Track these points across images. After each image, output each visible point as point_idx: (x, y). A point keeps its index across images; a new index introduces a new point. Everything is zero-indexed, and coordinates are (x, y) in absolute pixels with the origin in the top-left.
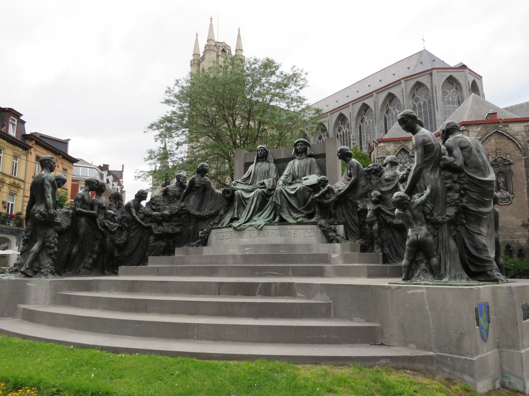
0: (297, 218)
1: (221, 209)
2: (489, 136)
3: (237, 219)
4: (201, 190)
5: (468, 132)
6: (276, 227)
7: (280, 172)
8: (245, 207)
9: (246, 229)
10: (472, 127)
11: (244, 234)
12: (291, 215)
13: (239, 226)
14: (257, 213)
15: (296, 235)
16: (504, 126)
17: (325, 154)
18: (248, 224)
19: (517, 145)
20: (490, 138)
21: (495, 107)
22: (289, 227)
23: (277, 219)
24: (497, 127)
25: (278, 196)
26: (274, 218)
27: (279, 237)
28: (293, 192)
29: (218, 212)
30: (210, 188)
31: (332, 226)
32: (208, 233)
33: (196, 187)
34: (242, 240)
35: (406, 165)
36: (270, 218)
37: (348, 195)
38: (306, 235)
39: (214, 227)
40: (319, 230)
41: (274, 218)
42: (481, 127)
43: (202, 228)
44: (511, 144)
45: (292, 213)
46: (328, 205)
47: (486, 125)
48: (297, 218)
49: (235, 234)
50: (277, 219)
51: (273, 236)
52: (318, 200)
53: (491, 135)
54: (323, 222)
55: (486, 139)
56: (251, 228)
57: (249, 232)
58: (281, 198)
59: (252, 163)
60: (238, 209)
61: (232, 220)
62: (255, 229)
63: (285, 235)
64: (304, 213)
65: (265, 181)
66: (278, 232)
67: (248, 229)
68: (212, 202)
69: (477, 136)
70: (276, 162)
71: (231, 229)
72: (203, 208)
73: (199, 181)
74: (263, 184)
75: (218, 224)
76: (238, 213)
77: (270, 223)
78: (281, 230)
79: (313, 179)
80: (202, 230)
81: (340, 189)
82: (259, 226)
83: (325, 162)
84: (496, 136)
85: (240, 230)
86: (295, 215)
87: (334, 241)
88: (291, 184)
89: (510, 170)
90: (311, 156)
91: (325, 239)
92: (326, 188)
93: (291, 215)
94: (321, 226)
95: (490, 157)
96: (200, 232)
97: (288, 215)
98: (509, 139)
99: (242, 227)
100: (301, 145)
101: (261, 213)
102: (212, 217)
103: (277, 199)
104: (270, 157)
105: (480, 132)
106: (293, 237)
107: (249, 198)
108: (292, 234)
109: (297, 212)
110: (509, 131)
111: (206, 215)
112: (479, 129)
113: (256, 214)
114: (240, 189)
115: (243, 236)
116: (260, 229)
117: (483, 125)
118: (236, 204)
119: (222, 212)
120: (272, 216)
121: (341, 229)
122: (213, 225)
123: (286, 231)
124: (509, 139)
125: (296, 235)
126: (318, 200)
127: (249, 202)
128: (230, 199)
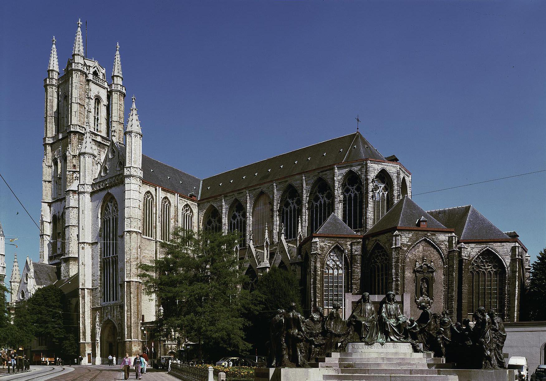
6: (392, 343)
7: (379, 312)
16: (432, 235)
19: (440, 254)
20: (418, 245)
21: (425, 215)
23: (389, 340)
24: (426, 234)
26: (387, 339)
35: (338, 263)
41: (387, 339)
42: (413, 232)
44: (436, 253)
50: (389, 340)
53: (420, 242)
77: (387, 342)
84: (424, 243)
89: (432, 277)
94: (412, 344)
95: (417, 263)
96: (339, 344)
98: (435, 248)
102: (344, 335)
109: (398, 335)
110: (435, 240)
112: (411, 235)
124: (435, 248)
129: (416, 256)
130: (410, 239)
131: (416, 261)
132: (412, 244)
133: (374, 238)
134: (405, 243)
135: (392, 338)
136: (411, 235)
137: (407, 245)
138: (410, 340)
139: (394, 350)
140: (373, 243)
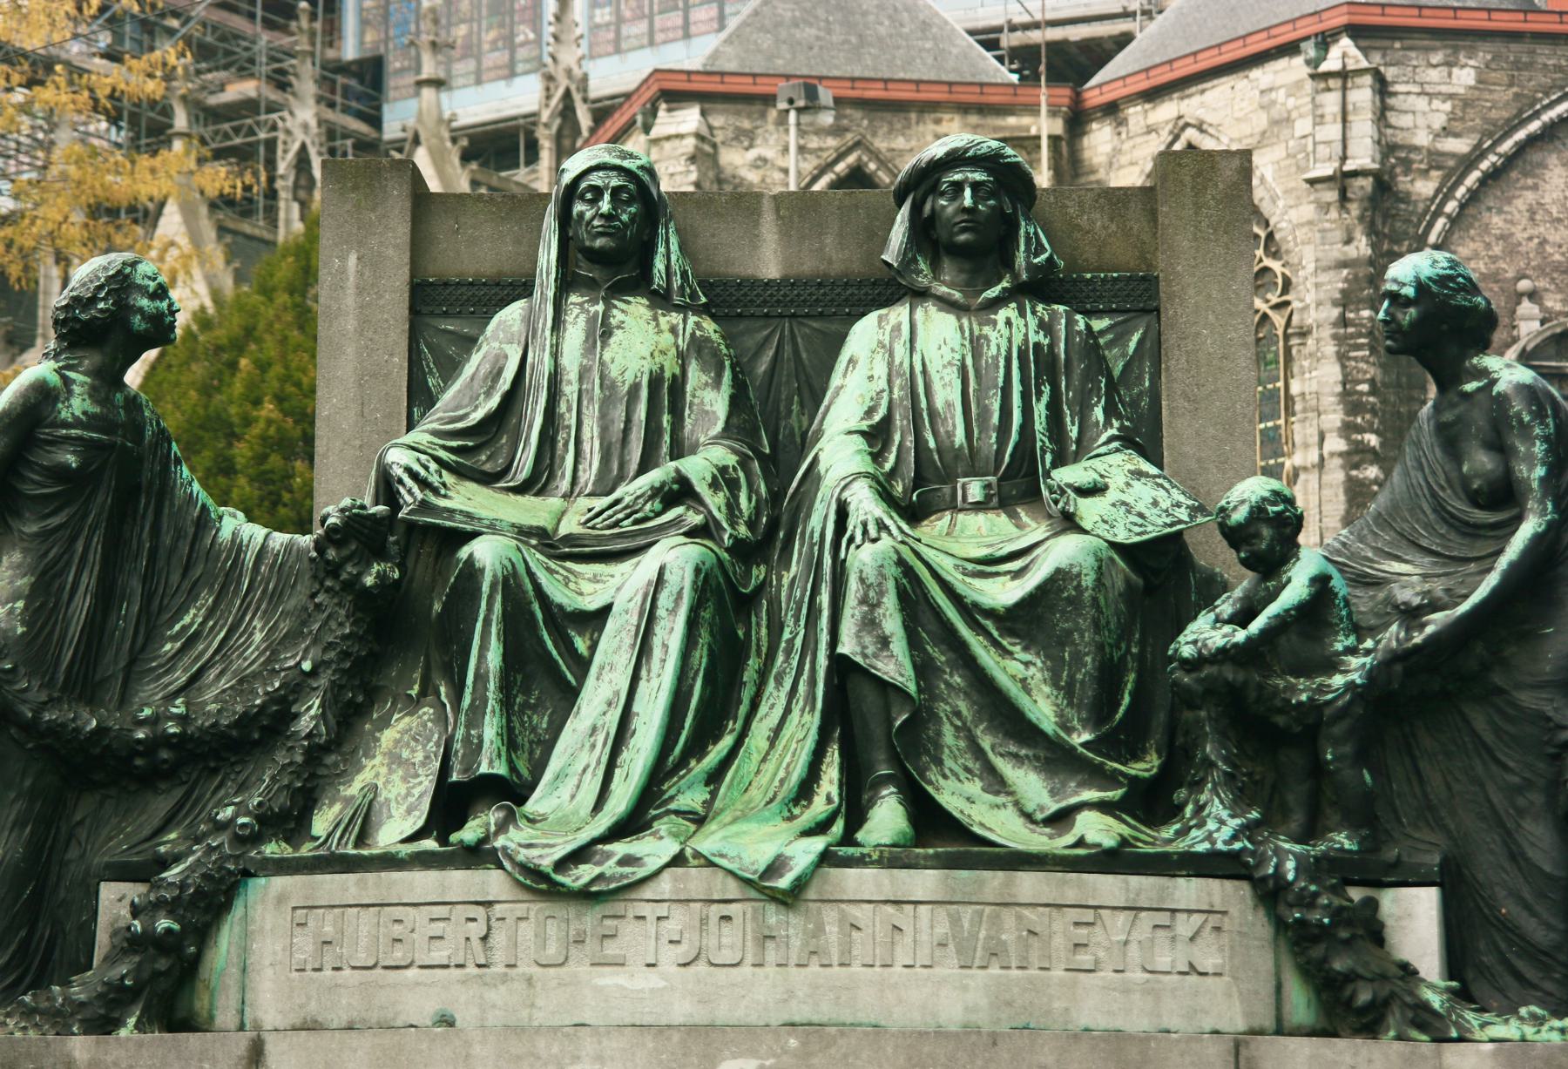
0: (1061, 819)
1: (298, 686)
2: (1532, 140)
3: (511, 792)
4: (103, 499)
5: (1382, 88)
6: (924, 882)
8: (570, 695)
9: (648, 892)
10: (1415, 58)
11: (628, 928)
12: (997, 783)
13: (579, 855)
14: (697, 748)
15: (1085, 959)
17: (1149, 284)
18: (654, 848)
20: (1535, 156)
22: (1028, 884)
25: (892, 623)
27: (949, 969)
28: (1002, 592)
29: (278, 716)
30: (164, 486)
31: (1356, 894)
32: (212, 901)
33: (60, 473)
34: (609, 979)
36: (819, 807)
37: (1479, 648)
38: (1163, 961)
39: (271, 849)
40: (1259, 925)
41: (855, 810)
42: (1483, 55)
43: (118, 847)
45: (1005, 767)
46: (1314, 718)
47: (1515, 50)
48: (1061, 819)
49: (533, 929)
50: (887, 818)
51: (902, 957)
52: (1229, 673)
54: (1287, 857)
55: (1511, 160)
56: (695, 880)
57: (678, 912)
58: (913, 642)
59: (523, 288)
60: (506, 703)
61: (451, 803)
62: (733, 889)
63: (995, 953)
64: (1111, 779)
65: (697, 467)
66: (929, 925)
67: (665, 886)
68: (191, 618)
69: (1446, 132)
70: (727, 299)
71: (492, 882)
72: (113, 663)
73: (90, 421)
74: (680, 492)
75: (289, 821)
76: (510, 741)
78: (967, 913)
79: (1123, 498)
80: (145, 870)
81: (1408, 595)
82: (776, 867)
83: (1153, 350)
85: (586, 896)
86: (1032, 786)
87: (1394, 1019)
88: (914, 513)
90: (1040, 288)
91: (1300, 1003)
92: (1295, 589)
93: (997, 783)
94: (1271, 894)
96: (115, 901)
97: (974, 787)
99: (609, 868)
100: (975, 186)
101: (727, 741)
103: (884, 642)
104: (667, 259)
105: (1466, 103)
106: (1058, 973)
107: (606, 610)
108: (1058, 941)
109: (1055, 758)
111: (166, 740)
112: (1464, 77)
113: (683, 762)
114: (493, 528)
115: (611, 949)
116: (776, 892)
117: (1498, 46)
118: (494, 658)
119: (309, 715)
120: (830, 781)
121: (1415, 921)
122: (256, 839)
123: (1008, 917)
125: (1085, 959)
126: (1229, 673)
127: (613, 651)
128: (398, 603)
129: (1512, 251)
130: (1465, 103)
131: (1519, 296)
132: (1478, 154)
133: (1167, 110)
134: (1422, 139)
135: (957, 794)
136: (1464, 77)
137: (1435, 159)
138: (1217, 824)
139: (952, 996)
140: (1157, 144)
